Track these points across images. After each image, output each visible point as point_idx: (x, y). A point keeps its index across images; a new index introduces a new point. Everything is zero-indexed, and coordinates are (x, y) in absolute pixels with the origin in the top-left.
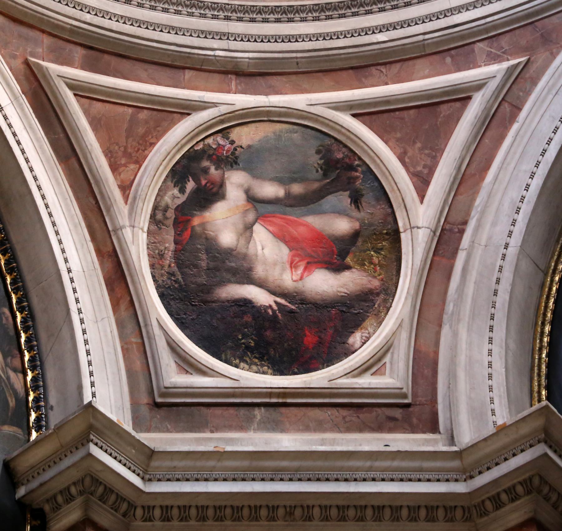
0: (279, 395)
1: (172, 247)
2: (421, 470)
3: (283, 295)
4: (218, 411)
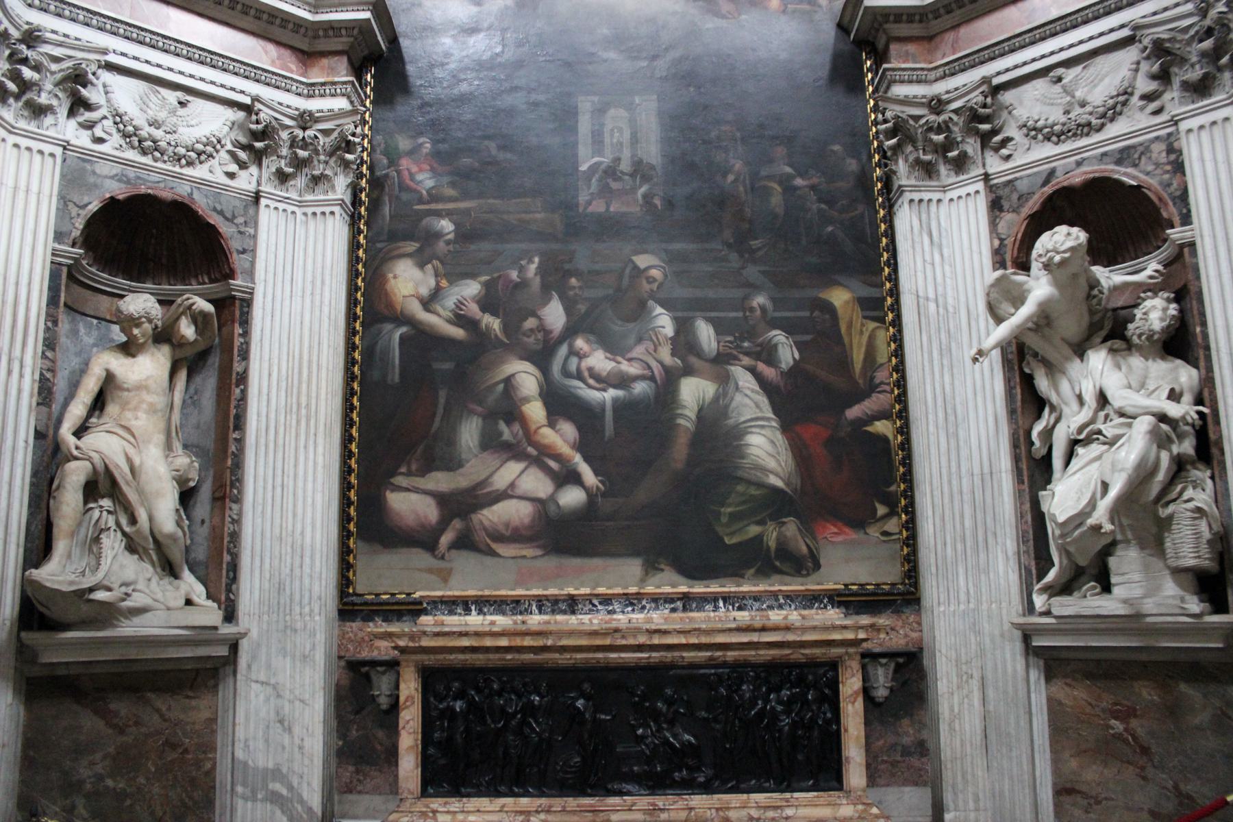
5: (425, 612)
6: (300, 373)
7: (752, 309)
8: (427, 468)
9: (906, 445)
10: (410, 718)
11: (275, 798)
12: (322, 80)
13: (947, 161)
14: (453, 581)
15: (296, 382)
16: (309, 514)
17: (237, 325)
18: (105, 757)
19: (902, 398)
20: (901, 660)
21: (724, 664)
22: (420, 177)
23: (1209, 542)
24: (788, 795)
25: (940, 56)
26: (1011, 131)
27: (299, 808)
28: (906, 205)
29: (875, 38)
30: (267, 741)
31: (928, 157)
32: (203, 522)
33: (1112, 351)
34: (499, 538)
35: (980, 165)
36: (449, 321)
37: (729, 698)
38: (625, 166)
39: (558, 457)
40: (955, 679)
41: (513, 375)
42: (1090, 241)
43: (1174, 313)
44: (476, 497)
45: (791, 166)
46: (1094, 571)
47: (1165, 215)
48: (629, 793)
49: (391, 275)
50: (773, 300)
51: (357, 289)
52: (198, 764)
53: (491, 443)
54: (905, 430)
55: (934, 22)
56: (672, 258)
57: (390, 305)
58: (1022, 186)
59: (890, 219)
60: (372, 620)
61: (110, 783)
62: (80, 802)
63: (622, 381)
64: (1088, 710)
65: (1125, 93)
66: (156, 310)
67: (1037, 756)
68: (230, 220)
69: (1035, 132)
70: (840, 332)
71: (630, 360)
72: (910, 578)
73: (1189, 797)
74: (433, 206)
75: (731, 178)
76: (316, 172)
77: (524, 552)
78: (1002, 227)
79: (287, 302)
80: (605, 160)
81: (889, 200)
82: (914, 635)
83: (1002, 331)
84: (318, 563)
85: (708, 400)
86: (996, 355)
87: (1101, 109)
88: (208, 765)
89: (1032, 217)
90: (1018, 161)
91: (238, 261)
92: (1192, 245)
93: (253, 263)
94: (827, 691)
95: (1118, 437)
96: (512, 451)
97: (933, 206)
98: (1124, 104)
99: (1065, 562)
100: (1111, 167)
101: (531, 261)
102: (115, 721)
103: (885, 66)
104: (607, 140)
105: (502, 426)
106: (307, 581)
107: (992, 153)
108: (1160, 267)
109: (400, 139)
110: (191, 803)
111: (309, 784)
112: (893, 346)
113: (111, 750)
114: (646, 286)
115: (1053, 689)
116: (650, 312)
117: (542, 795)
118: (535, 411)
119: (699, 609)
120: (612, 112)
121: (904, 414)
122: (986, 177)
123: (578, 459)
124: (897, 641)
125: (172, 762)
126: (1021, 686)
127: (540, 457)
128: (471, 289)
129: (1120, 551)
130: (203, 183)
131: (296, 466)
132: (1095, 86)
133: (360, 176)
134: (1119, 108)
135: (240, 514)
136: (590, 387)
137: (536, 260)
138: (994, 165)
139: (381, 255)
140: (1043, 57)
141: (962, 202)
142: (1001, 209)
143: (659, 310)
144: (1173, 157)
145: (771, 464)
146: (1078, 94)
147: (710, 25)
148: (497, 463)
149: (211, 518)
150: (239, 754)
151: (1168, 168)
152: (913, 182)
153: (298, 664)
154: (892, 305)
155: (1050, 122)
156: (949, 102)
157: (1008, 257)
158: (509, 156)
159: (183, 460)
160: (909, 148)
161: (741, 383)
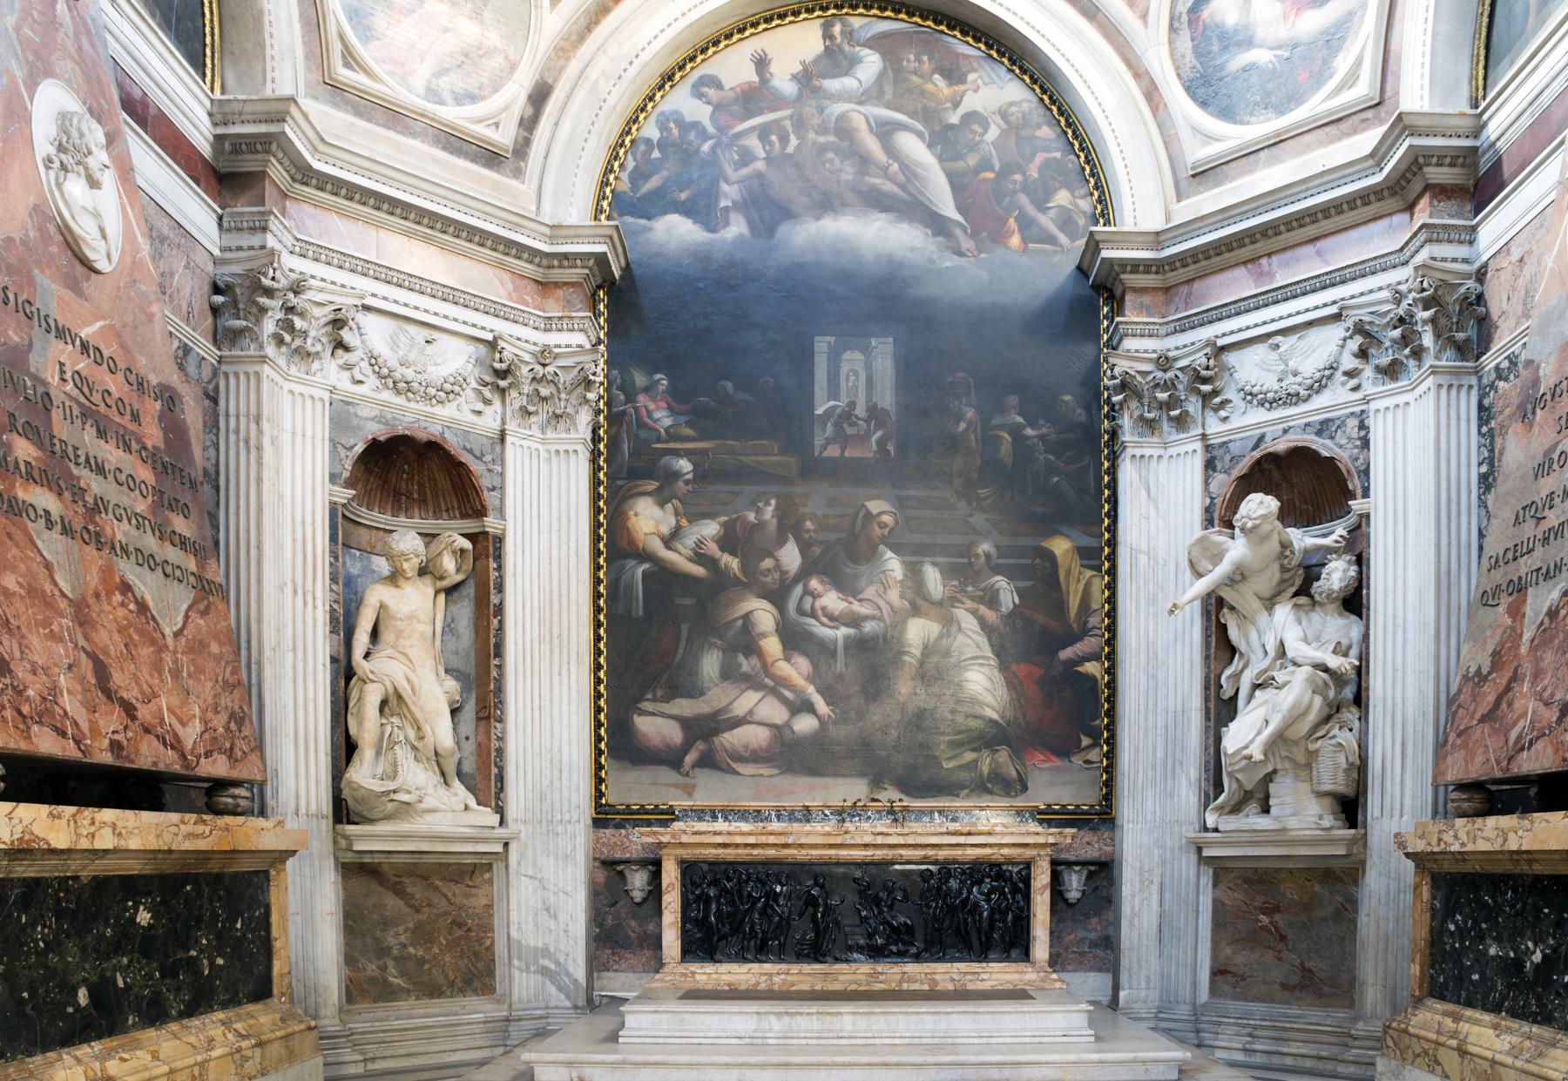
0: (1274, 137)
1: (1189, 45)
2: (1345, 176)
3: (1280, 47)
4: (1233, 164)
5: (677, 819)
6: (551, 606)
7: (977, 555)
8: (676, 690)
9: (1112, 685)
10: (672, 901)
11: (544, 972)
12: (560, 314)
13: (1170, 419)
14: (697, 794)
15: (548, 614)
16: (565, 734)
17: (491, 560)
18: (406, 930)
19: (1111, 642)
20: (1092, 868)
21: (935, 863)
22: (657, 415)
23: (1345, 771)
24: (984, 965)
25: (1173, 310)
26: (1230, 394)
27: (567, 980)
28: (1128, 461)
29: (1113, 285)
30: (536, 924)
31: (1151, 416)
32: (467, 738)
33: (1296, 606)
34: (739, 758)
35: (1200, 424)
36: (690, 560)
37: (939, 889)
38: (860, 411)
39: (791, 687)
40: (1137, 885)
41: (751, 612)
42: (1281, 509)
43: (1353, 574)
44: (717, 722)
45: (1020, 414)
46: (1261, 796)
47: (1350, 486)
48: (855, 961)
49: (632, 513)
50: (997, 546)
51: (600, 525)
52: (480, 941)
53: (729, 674)
54: (1111, 671)
55: (1170, 275)
56: (901, 503)
57: (632, 542)
58: (1235, 448)
59: (1113, 471)
60: (624, 827)
61: (412, 950)
62: (391, 964)
63: (854, 621)
64: (1244, 908)
65: (1332, 368)
66: (418, 543)
67: (1200, 945)
68: (479, 458)
69: (1252, 397)
70: (1058, 578)
71: (860, 601)
72: (1106, 800)
73: (1310, 971)
74: (671, 445)
75: (963, 426)
76: (558, 412)
77: (761, 771)
78: (1213, 487)
79: (535, 538)
80: (841, 404)
81: (1114, 453)
82: (1108, 849)
83: (1202, 585)
84: (575, 777)
85: (932, 640)
86: (1197, 604)
87: (1309, 381)
88: (488, 943)
89: (1241, 478)
90: (1236, 422)
91: (490, 499)
92: (1368, 516)
93: (502, 500)
94: (1021, 885)
95: (1286, 684)
96: (751, 682)
97: (1154, 463)
98: (1329, 377)
99: (1235, 786)
100: (1313, 437)
101: (767, 503)
102: (412, 902)
103: (1118, 319)
104: (843, 383)
105: (741, 658)
106: (565, 792)
107: (1212, 413)
108: (1344, 533)
109: (636, 374)
110: (475, 972)
111: (574, 961)
112: (1107, 593)
113: (411, 925)
114: (878, 531)
115: (1218, 892)
116: (882, 555)
117: (782, 961)
118: (772, 646)
119: (917, 820)
120: (848, 355)
121: (1112, 657)
122: (1204, 436)
123: (811, 690)
124: (1092, 853)
125: (460, 938)
126: (1192, 888)
127: (776, 687)
128: (710, 529)
129: (1278, 778)
130: (453, 420)
131: (551, 690)
132: (1306, 358)
133: (598, 412)
134: (1323, 382)
135: (504, 732)
136: (823, 624)
137: (773, 502)
138: (1214, 426)
139: (621, 493)
140: (1265, 323)
141: (1181, 459)
142: (1214, 470)
143: (889, 554)
144: (1363, 433)
145: (989, 699)
146: (1291, 363)
147: (948, 264)
148: (736, 692)
149: (477, 735)
150: (514, 934)
151: (1358, 443)
152: (1136, 439)
153: (561, 862)
154: (1109, 555)
155: (1264, 388)
156: (1176, 359)
157: (1216, 516)
158: (746, 396)
159: (452, 684)
160: (1134, 404)
161: (963, 625)
